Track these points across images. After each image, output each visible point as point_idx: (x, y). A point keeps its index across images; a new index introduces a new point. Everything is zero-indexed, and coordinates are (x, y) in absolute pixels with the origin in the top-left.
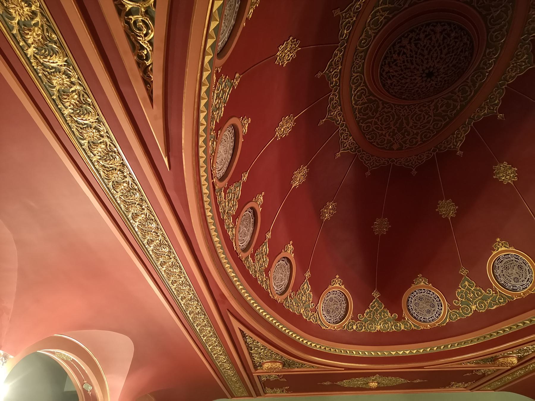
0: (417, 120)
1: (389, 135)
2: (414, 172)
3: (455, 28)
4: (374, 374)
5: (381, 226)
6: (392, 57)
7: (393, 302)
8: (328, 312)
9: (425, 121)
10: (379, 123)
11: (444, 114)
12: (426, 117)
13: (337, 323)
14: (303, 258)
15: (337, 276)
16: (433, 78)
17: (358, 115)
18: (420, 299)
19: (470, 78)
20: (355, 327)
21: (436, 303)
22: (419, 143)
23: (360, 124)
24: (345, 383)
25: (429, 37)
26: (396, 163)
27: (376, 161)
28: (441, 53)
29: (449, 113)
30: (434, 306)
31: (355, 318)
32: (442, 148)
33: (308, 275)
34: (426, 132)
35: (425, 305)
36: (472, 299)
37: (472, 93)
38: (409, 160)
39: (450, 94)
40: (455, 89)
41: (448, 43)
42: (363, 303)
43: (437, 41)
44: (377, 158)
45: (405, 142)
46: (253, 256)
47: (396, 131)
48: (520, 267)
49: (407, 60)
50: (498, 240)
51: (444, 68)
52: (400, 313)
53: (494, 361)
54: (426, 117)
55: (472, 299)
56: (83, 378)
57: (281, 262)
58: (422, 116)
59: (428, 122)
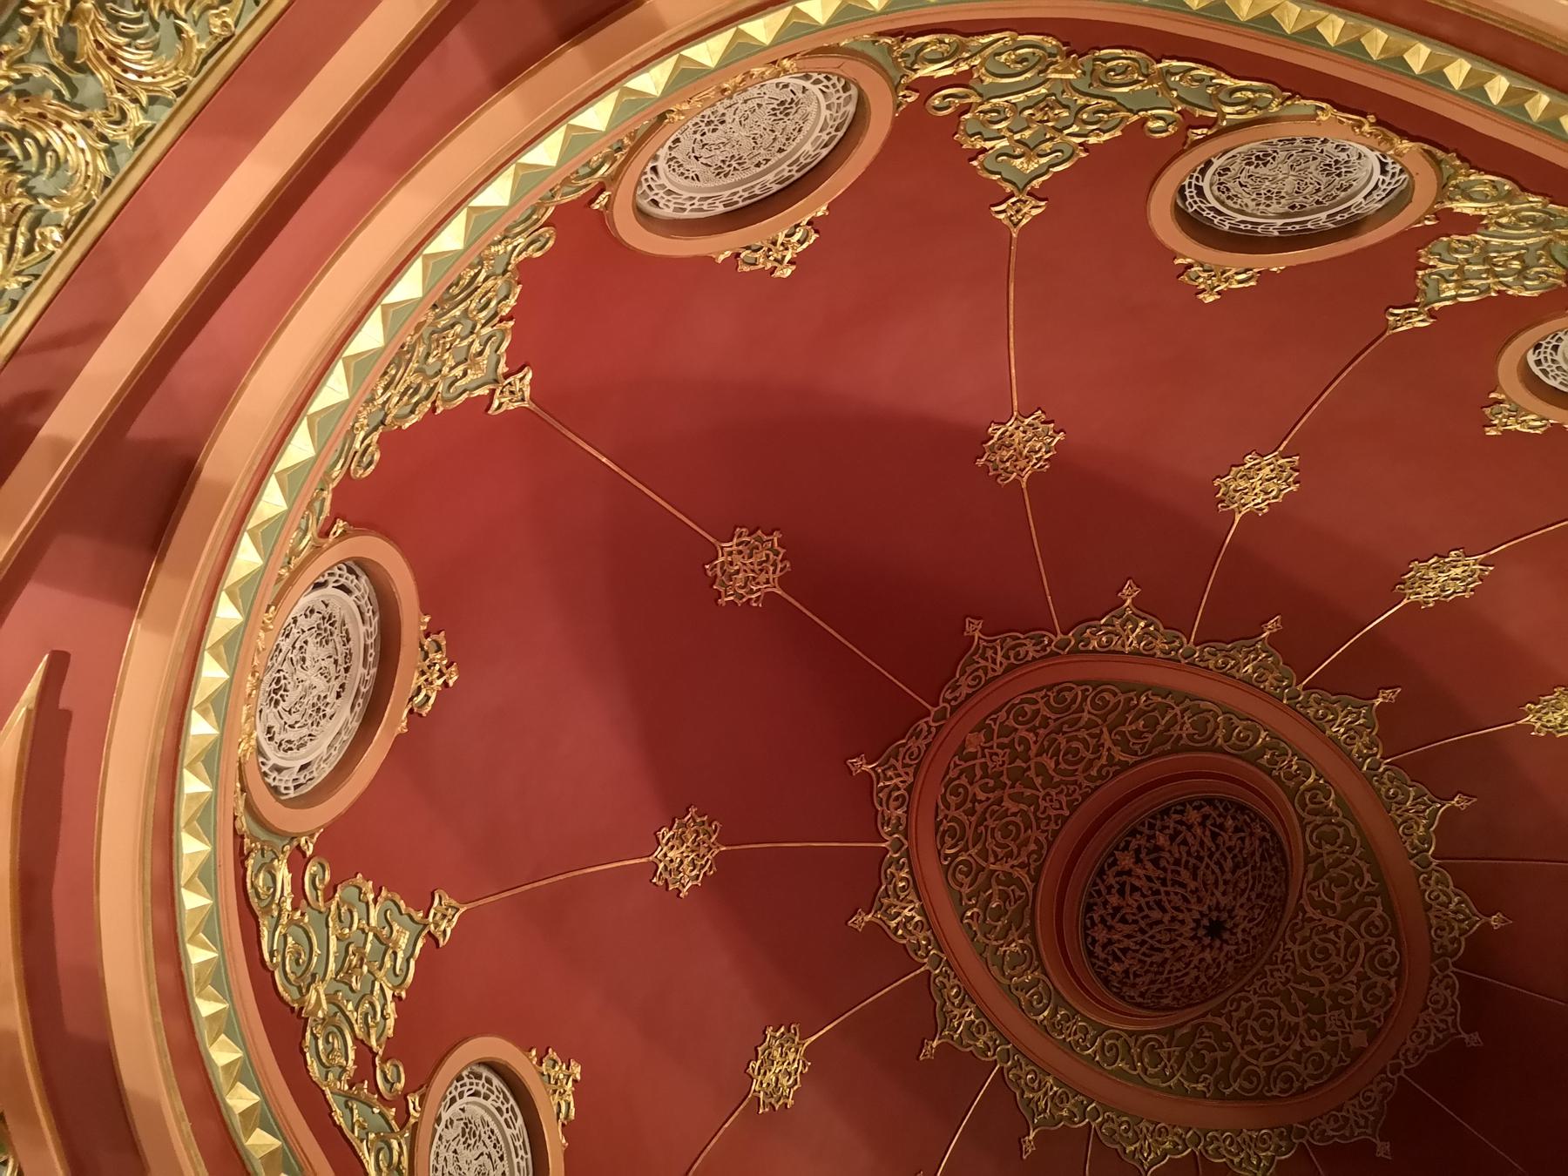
0: (1320, 960)
1: (1314, 1038)
2: (1473, 1039)
3: (1152, 827)
6: (1114, 973)
9: (1342, 944)
10: (1260, 1045)
11: (1354, 900)
12: (1331, 935)
16: (1226, 936)
17: (1200, 1087)
19: (1304, 815)
22: (1392, 985)
23: (1227, 1092)
25: (1128, 889)
26: (1408, 1062)
27: (1362, 1107)
28: (1183, 885)
29: (1362, 889)
32: (1450, 948)
34: (1373, 957)
37: (1351, 827)
38: (1424, 1032)
39: (1312, 866)
40: (1307, 851)
41: (1171, 860)
43: (1149, 879)
44: (1355, 1102)
45: (1362, 1013)
47: (1315, 1018)
49: (1144, 954)
51: (1224, 893)
54: (1331, 935)
58: (1321, 944)
59: (1350, 939)
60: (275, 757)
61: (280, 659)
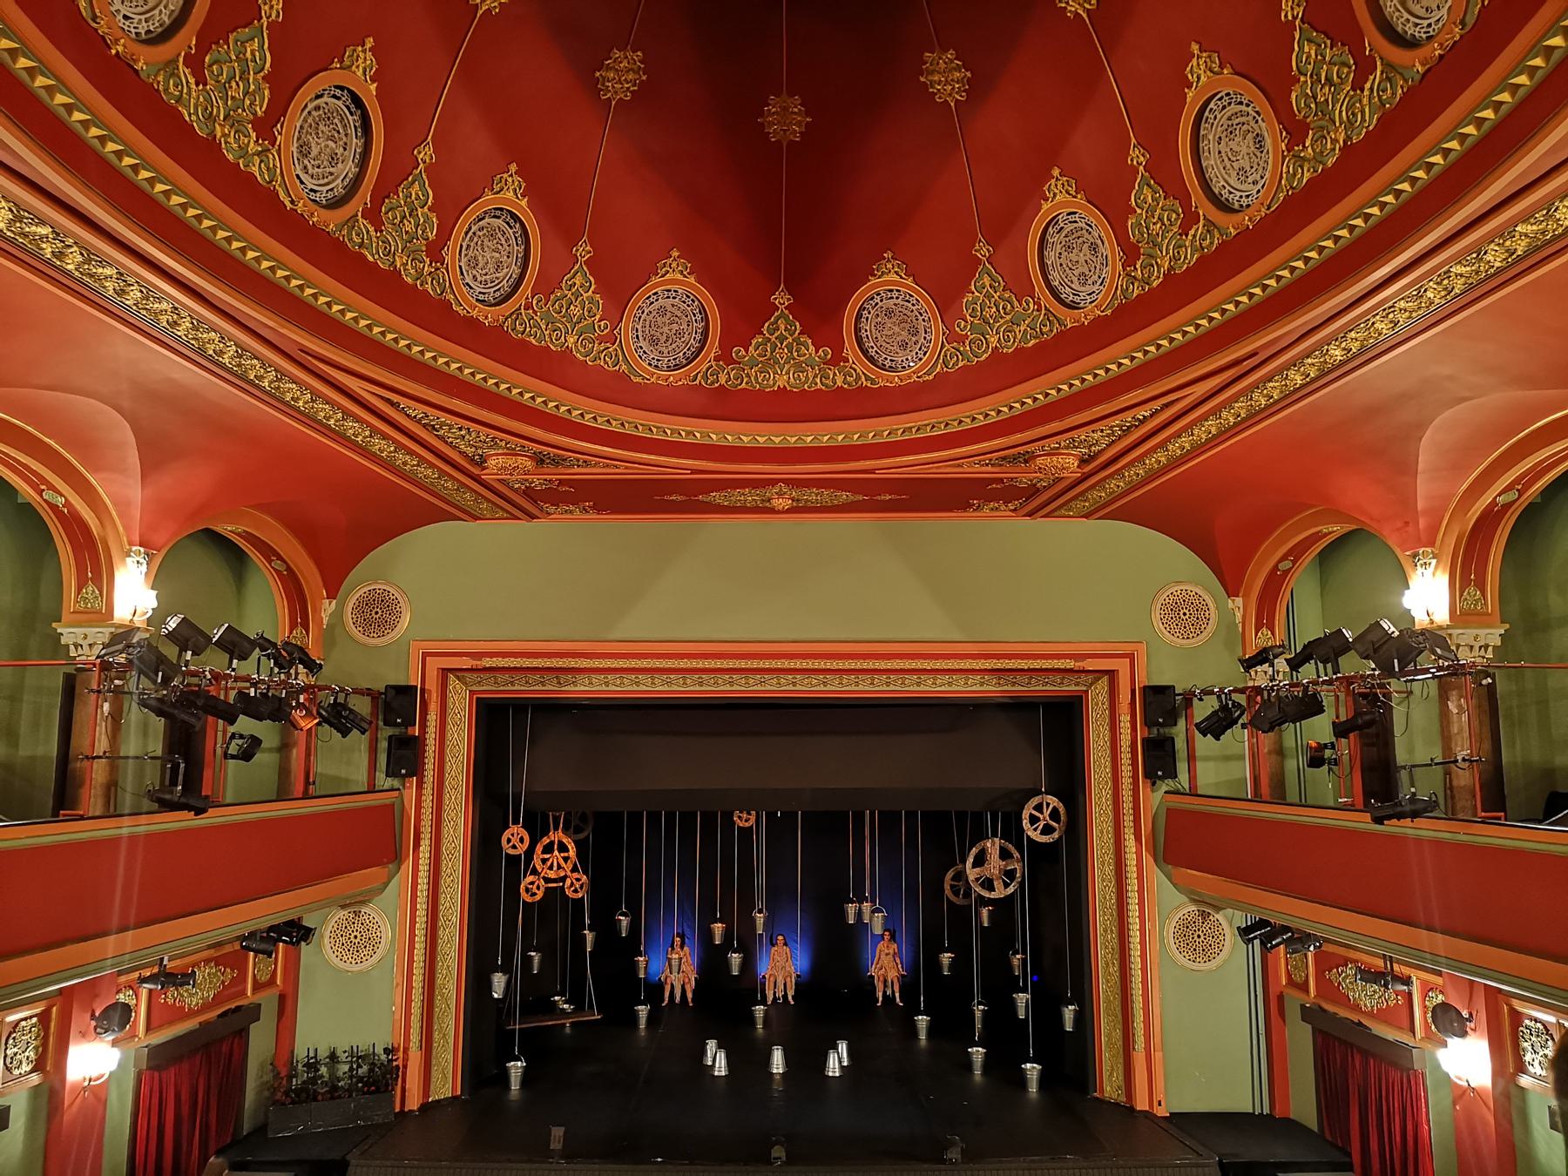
4: (773, 482)
5: (785, 119)
7: (821, 319)
8: (654, 342)
13: (677, 367)
14: (559, 210)
15: (675, 253)
18: (889, 313)
20: (723, 380)
24: (716, 497)
30: (916, 333)
31: (725, 357)
33: (583, 250)
35: (897, 329)
36: (997, 320)
42: (743, 321)
46: (373, 215)
48: (1094, 248)
50: (1056, 172)
52: (838, 347)
53: (1026, 461)
55: (997, 320)
56: (38, 483)
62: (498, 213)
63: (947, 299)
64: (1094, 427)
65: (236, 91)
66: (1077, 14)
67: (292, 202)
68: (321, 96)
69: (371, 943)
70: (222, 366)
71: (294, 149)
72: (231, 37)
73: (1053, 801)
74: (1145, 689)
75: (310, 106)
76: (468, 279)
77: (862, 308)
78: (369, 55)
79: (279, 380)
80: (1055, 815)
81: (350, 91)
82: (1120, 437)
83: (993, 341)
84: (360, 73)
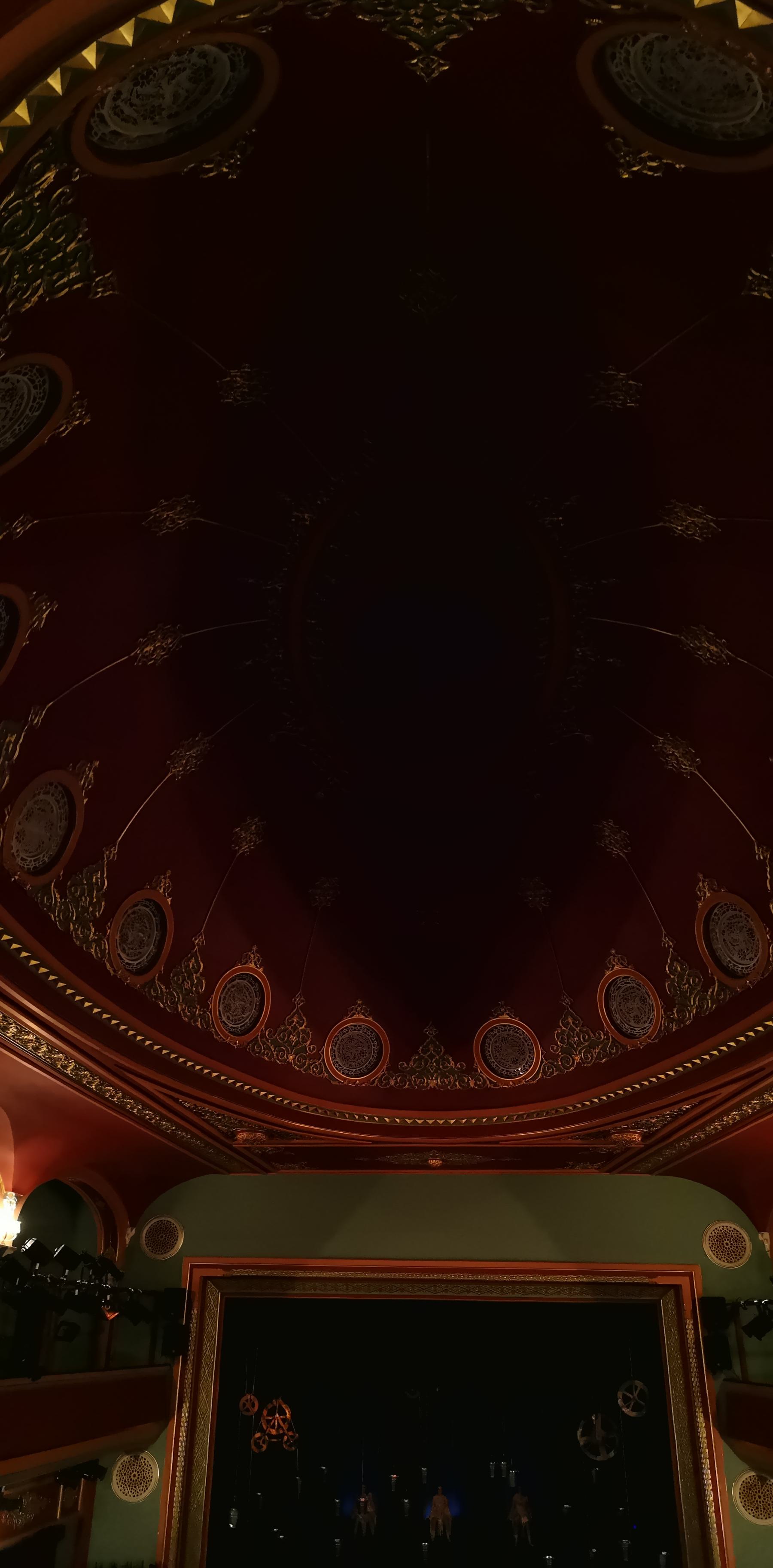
21: (526, 1048)
30: (524, 1053)
57: (237, 981)
60: (106, 111)
61: (164, 62)
62: (244, 976)
63: (544, 1033)
64: (652, 1114)
65: (85, 901)
66: (618, 855)
67: (114, 971)
68: (137, 905)
69: (145, 1480)
70: (66, 1075)
71: (117, 938)
72: (85, 871)
73: (638, 1383)
74: (702, 1300)
75: (130, 911)
76: (224, 1019)
77: (486, 1037)
78: (168, 880)
79: (102, 1084)
80: (641, 1394)
81: (154, 901)
82: (670, 1122)
83: (578, 1059)
84: (161, 891)
